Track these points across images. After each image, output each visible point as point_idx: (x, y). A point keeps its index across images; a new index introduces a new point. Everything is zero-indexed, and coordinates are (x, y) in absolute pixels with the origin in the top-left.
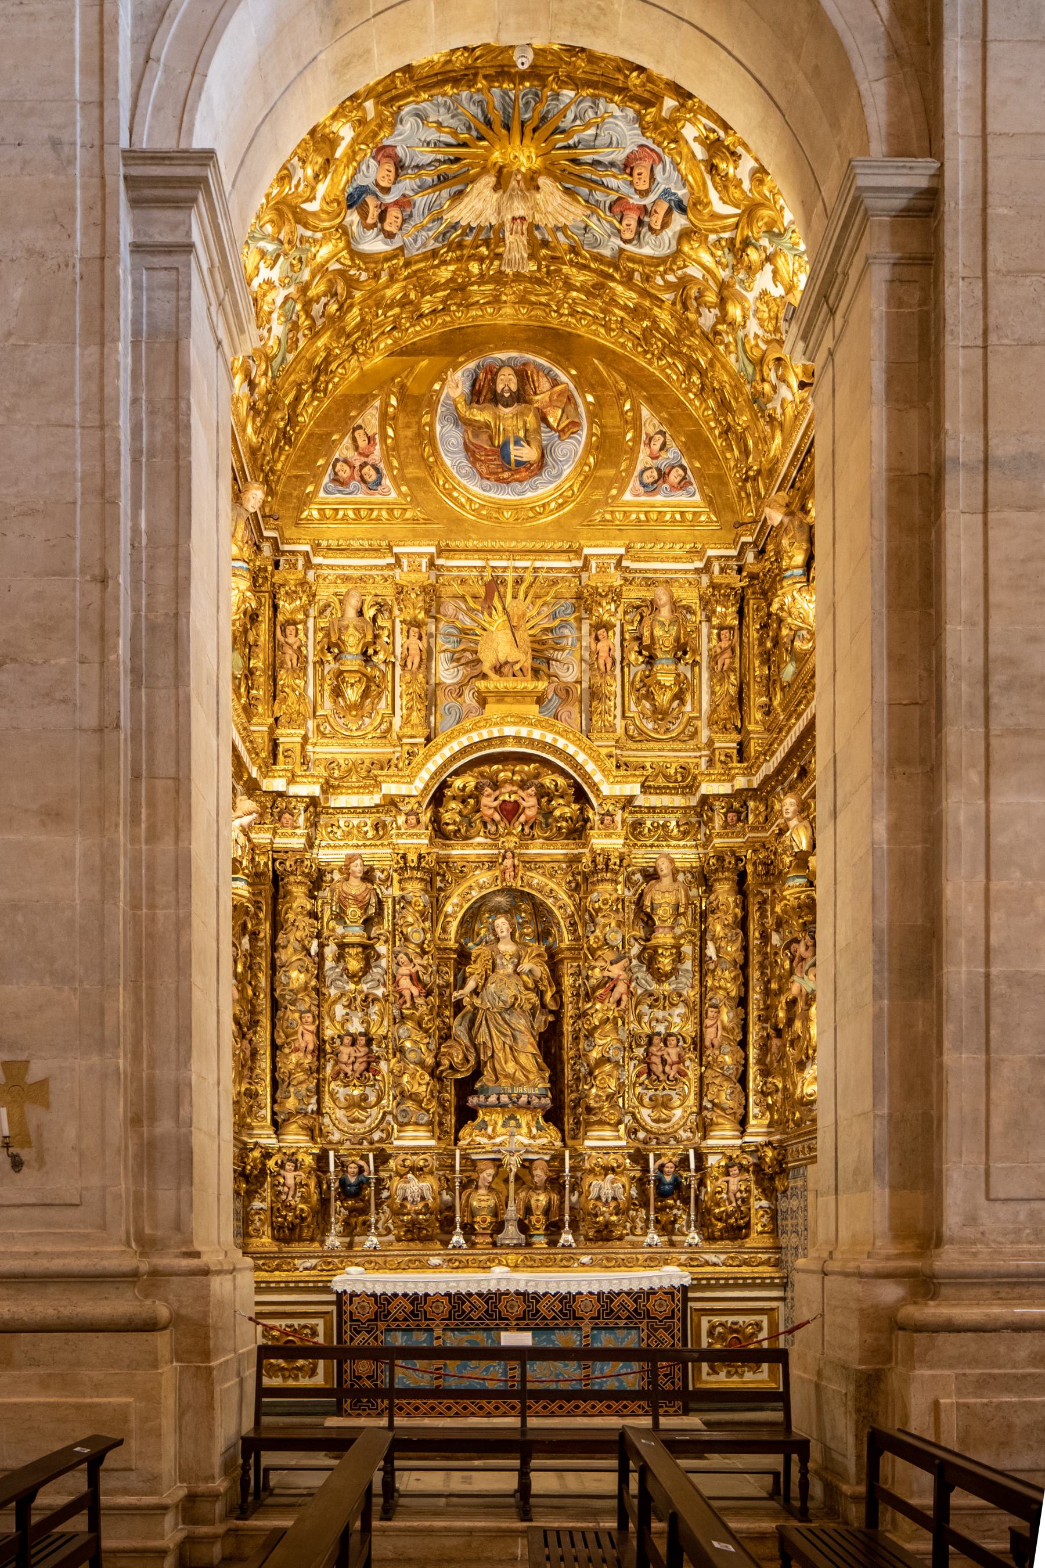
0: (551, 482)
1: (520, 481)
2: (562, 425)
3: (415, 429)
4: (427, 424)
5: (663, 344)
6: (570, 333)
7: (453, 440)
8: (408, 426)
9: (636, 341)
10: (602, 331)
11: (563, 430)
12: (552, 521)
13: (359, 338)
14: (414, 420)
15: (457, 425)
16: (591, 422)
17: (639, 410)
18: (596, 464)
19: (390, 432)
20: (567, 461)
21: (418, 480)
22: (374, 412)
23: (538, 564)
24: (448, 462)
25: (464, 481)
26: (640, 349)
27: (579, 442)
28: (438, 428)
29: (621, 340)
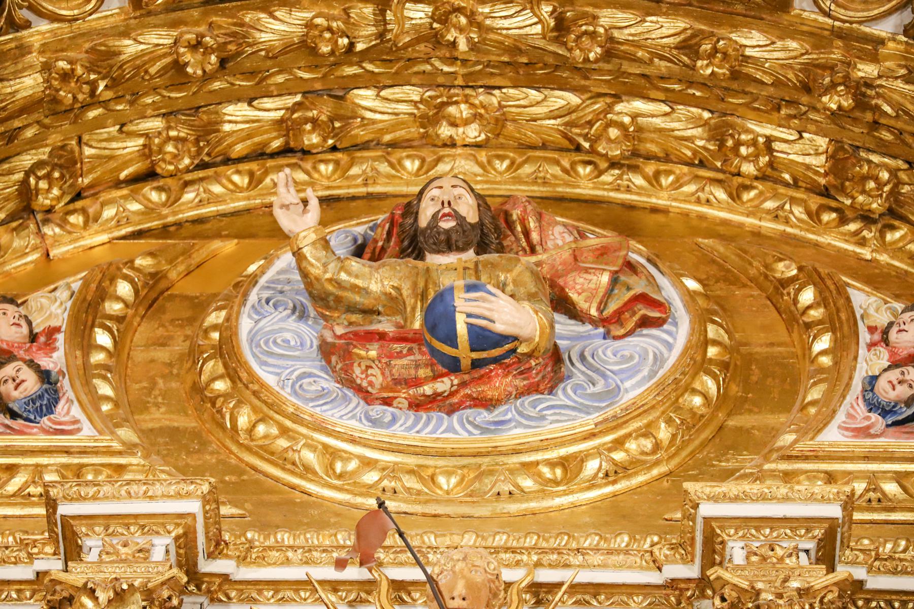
0: (586, 410)
1: (488, 404)
2: (613, 307)
3: (180, 346)
4: (215, 327)
5: (894, 172)
6: (630, 207)
7: (288, 336)
8: (162, 343)
9: (815, 202)
10: (721, 194)
11: (618, 317)
12: (593, 504)
13: (40, 164)
14: (179, 335)
15: (303, 315)
16: (702, 318)
17: (841, 290)
18: (723, 397)
19: (103, 338)
20: (634, 371)
21: (173, 433)
22: (62, 294)
23: (545, 576)
24: (270, 380)
25: (310, 409)
26: (826, 217)
27: (670, 347)
28: (245, 325)
29: (770, 205)
